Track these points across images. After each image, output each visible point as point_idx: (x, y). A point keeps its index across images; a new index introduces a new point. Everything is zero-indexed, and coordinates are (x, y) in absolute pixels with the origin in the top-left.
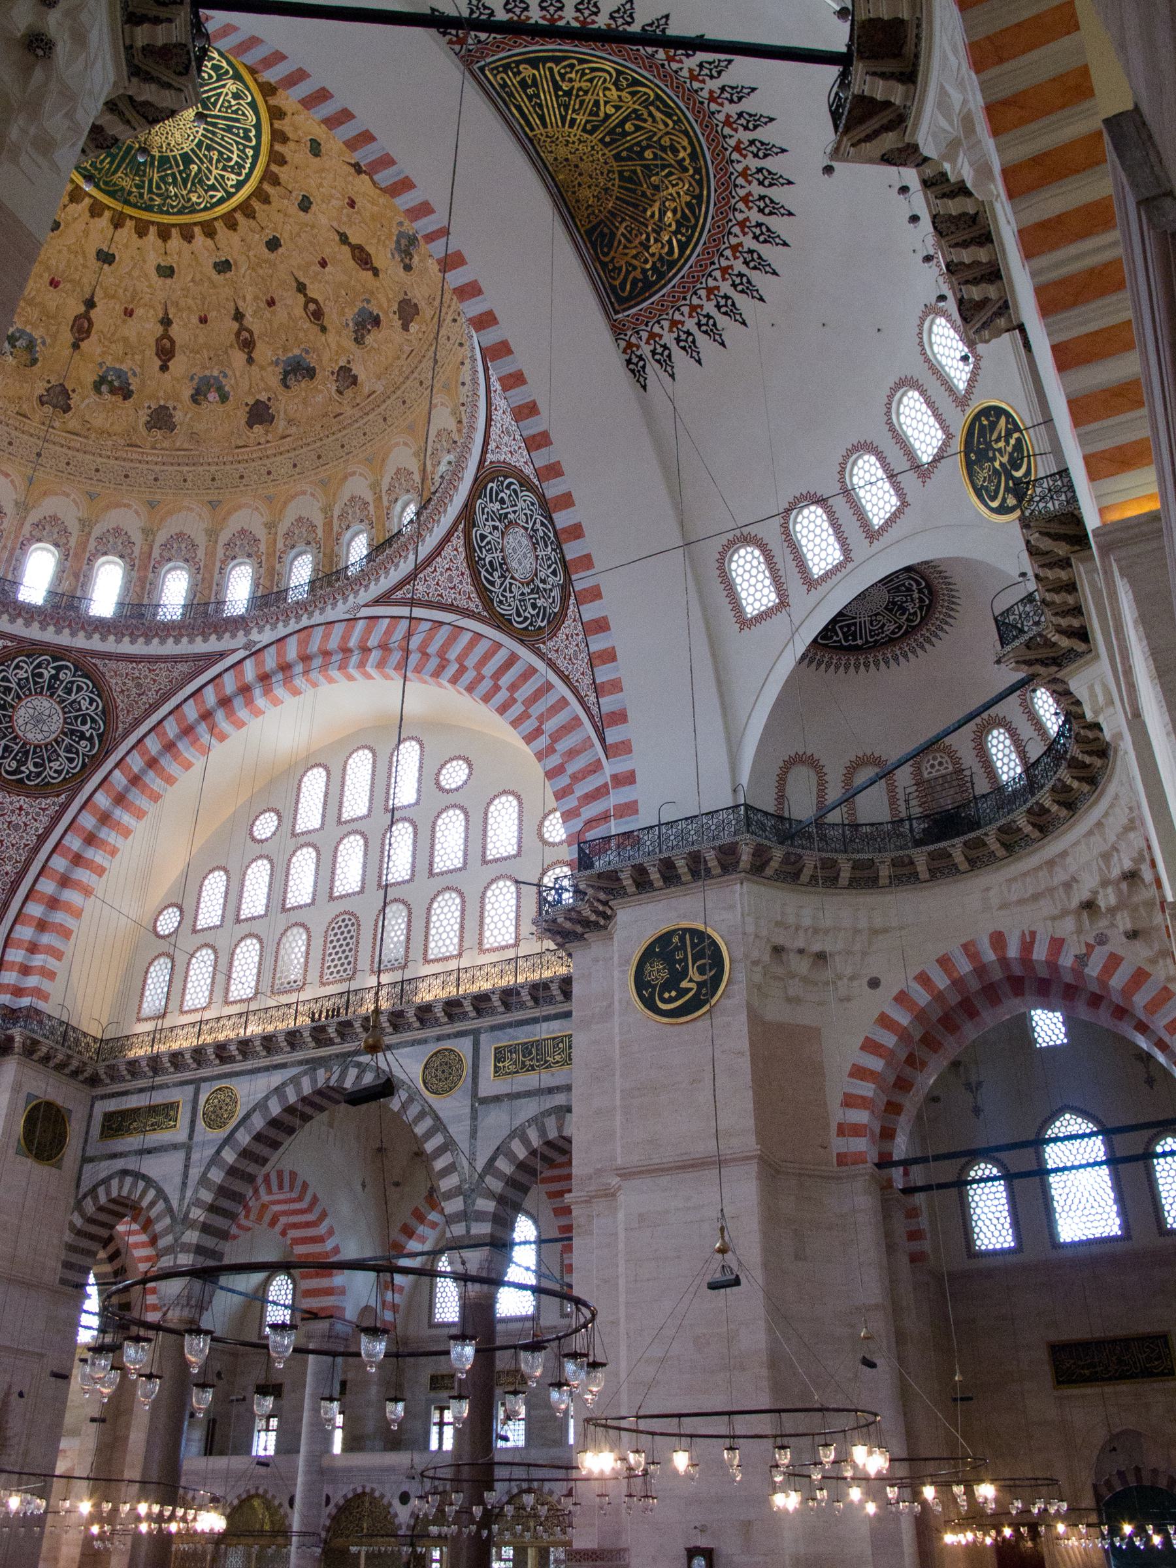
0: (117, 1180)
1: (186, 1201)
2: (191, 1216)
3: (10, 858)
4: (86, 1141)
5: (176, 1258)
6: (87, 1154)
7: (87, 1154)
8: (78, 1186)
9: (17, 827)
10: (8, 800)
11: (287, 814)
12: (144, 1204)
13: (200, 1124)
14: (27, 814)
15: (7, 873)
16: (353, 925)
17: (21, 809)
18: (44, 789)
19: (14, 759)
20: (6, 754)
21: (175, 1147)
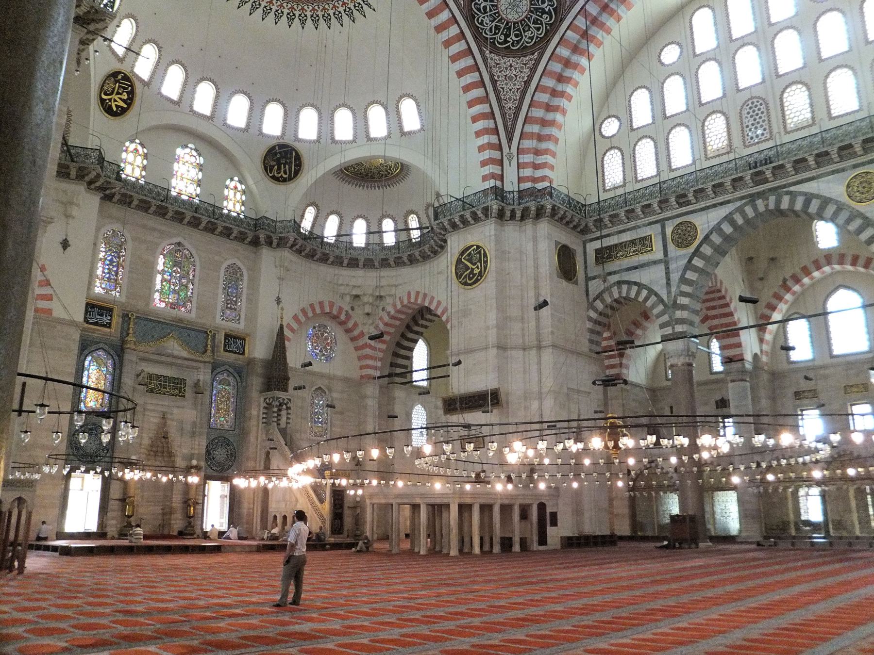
0: (616, 287)
1: (673, 294)
2: (678, 302)
3: (510, 99)
4: (586, 267)
5: (673, 328)
6: (589, 275)
7: (589, 275)
8: (587, 295)
9: (511, 79)
10: (503, 61)
11: (687, 44)
12: (641, 299)
13: (671, 247)
14: (516, 69)
15: (510, 108)
16: (761, 104)
17: (511, 66)
18: (524, 51)
19: (502, 34)
20: (497, 32)
21: (655, 262)
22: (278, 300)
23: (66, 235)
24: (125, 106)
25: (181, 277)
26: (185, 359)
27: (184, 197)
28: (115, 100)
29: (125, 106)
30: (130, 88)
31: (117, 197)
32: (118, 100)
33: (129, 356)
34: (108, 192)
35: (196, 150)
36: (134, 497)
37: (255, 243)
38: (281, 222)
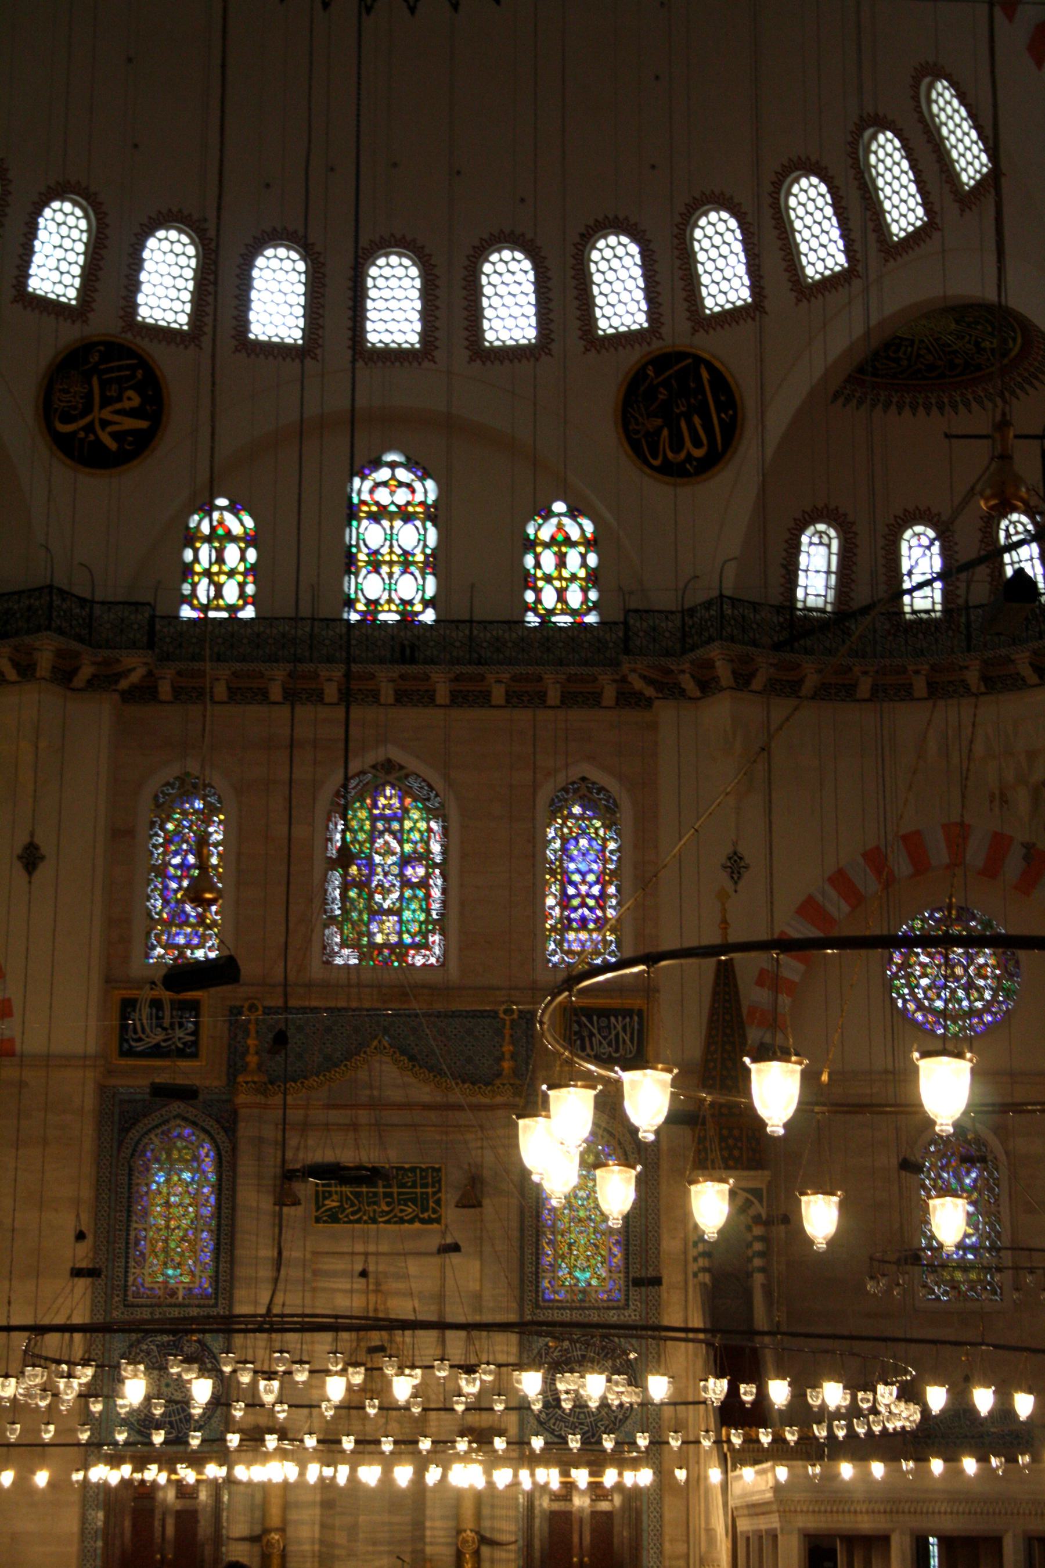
22: (735, 866)
23: (32, 835)
24: (143, 424)
25: (405, 861)
26: (427, 1107)
27: (389, 617)
28: (104, 424)
29: (143, 424)
30: (140, 374)
31: (165, 689)
32: (116, 418)
33: (245, 1130)
34: (124, 684)
35: (410, 465)
36: (282, 1530)
37: (629, 699)
38: (692, 611)
